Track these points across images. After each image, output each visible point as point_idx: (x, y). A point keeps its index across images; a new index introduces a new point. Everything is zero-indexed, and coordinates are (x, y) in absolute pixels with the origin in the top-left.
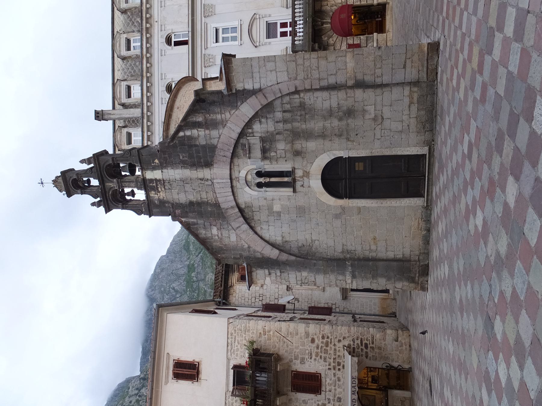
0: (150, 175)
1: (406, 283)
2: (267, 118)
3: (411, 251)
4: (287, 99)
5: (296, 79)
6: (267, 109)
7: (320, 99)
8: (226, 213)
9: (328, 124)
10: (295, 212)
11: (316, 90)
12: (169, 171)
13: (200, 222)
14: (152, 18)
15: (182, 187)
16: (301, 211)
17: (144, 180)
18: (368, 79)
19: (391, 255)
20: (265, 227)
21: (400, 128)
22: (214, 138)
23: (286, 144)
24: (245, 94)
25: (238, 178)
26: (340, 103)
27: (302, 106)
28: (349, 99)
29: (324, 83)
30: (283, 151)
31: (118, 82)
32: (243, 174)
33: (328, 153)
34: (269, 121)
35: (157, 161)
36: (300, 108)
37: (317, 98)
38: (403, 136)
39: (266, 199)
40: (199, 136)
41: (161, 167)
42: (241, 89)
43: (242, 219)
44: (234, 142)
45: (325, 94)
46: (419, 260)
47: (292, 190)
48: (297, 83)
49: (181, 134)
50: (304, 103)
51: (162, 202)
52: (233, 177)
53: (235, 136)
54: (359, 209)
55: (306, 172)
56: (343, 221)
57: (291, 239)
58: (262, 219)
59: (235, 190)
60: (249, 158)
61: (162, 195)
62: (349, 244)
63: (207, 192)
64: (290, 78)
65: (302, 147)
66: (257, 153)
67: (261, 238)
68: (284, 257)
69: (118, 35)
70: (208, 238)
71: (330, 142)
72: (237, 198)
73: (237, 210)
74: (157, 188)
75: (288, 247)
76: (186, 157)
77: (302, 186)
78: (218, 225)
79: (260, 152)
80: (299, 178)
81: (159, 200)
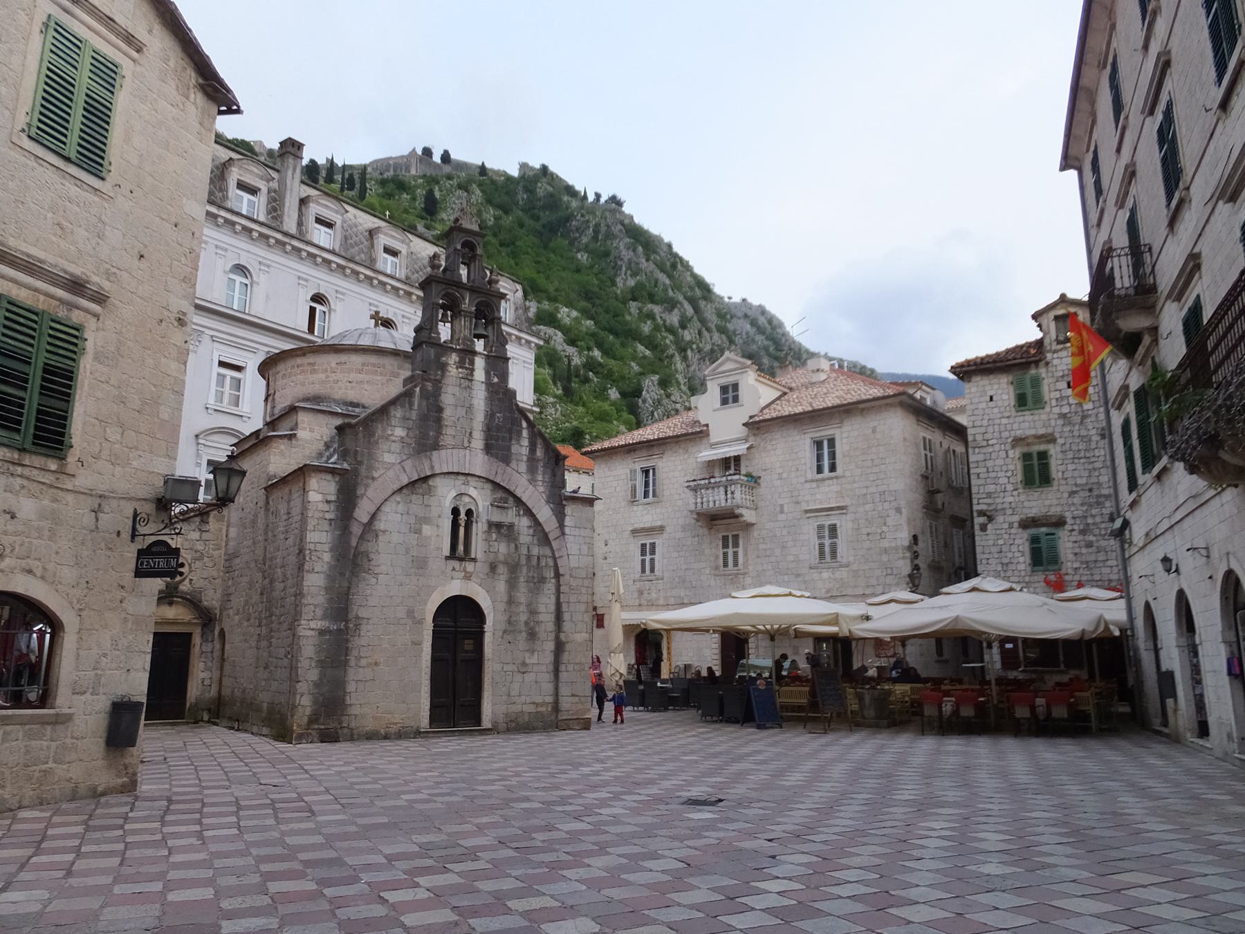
0: (480, 363)
1: (308, 711)
4: (551, 563)
6: (545, 539)
9: (522, 608)
11: (558, 598)
13: (414, 415)
16: (420, 564)
18: (565, 657)
20: (401, 508)
25: (466, 484)
27: (542, 580)
29: (564, 608)
35: (496, 380)
45: (552, 608)
48: (567, 577)
49: (524, 424)
51: (443, 367)
52: (469, 478)
53: (518, 493)
54: (417, 644)
56: (403, 621)
57: (381, 544)
61: (453, 371)
62: (370, 627)
66: (497, 517)
68: (356, 530)
70: (388, 419)
75: (369, 536)
78: (409, 441)
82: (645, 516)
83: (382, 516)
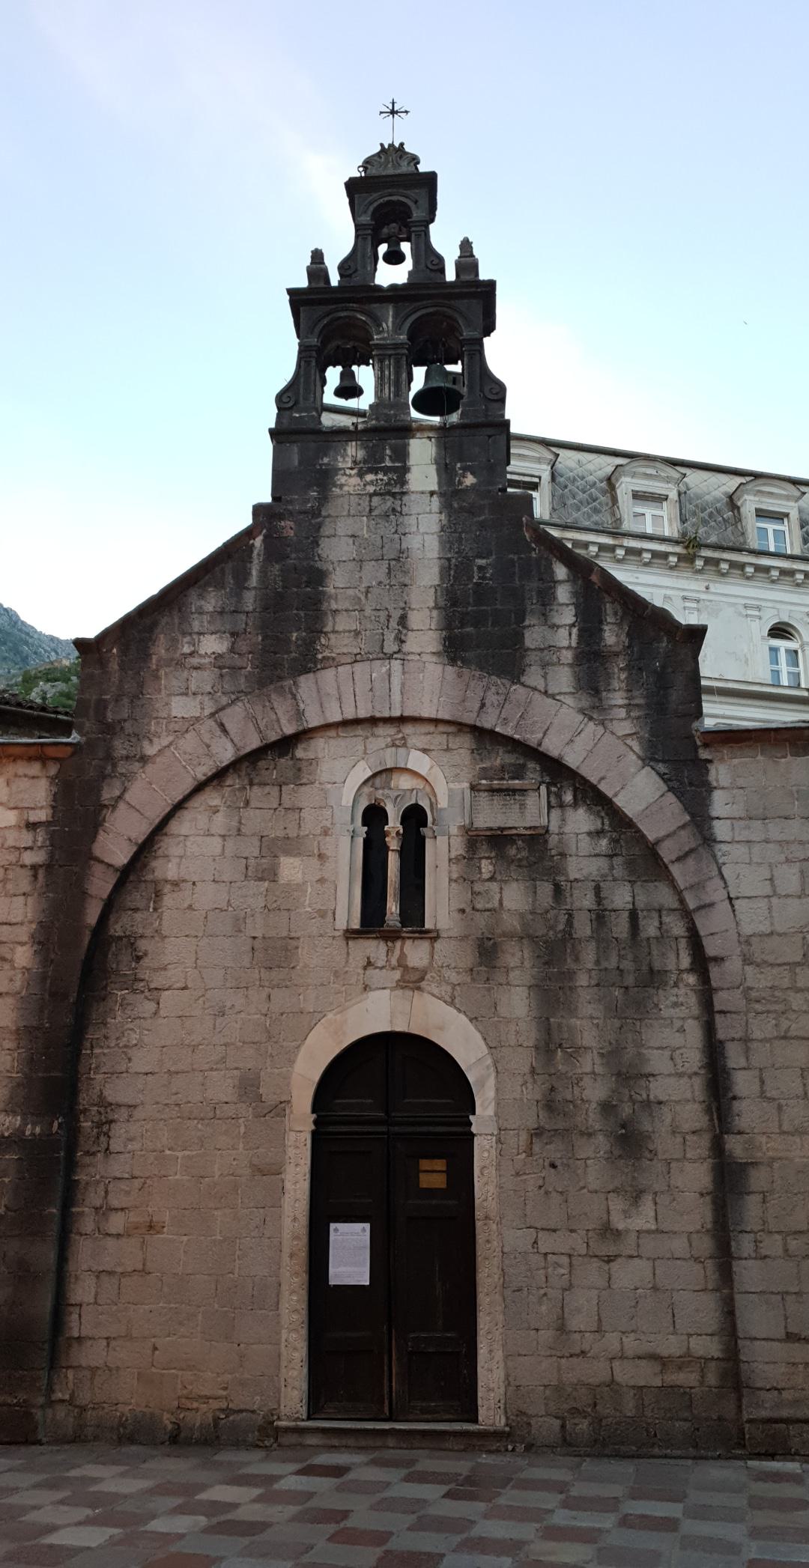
0: (422, 453)
2: (611, 856)
3: (94, 1370)
4: (678, 928)
5: (747, 960)
6: (643, 858)
7: (677, 1040)
8: (281, 691)
9: (589, 1063)
10: (272, 933)
12: (436, 517)
13: (249, 601)
14: (715, 578)
15: (378, 554)
16: (275, 955)
17: (408, 430)
19: (82, 1291)
21: (575, 1323)
22: (545, 677)
23: (522, 916)
26: (665, 1109)
27: (653, 978)
28: (679, 1139)
29: (734, 1057)
30: (497, 904)
31: (551, 457)
32: (418, 761)
33: (489, 1061)
34: (603, 863)
35: (470, 480)
36: (645, 968)
37: (682, 1030)
38: (547, 1335)
40: (555, 627)
41: (449, 494)
42: (712, 777)
43: (254, 743)
44: (532, 739)
45: (693, 1057)
46: (51, 1403)
47: (356, 924)
48: (734, 965)
49: (561, 572)
50: (663, 984)
51: (324, 479)
52: (408, 729)
53: (552, 746)
54: (271, 1171)
55: (422, 979)
56: (229, 1110)
57: (166, 916)
58: (248, 813)
59: (359, 731)
60: (473, 788)
61: (349, 482)
63: (357, 633)
64: (748, 943)
65: (507, 970)
66: (492, 815)
67: (179, 806)
69: (677, 475)
70: (184, 619)
71: (526, 1069)
72: (332, 733)
73: (289, 729)
74: (374, 471)
75: (136, 897)
76: (483, 578)
77: (369, 964)
79: (495, 825)
80: (397, 952)
83: (169, 846)
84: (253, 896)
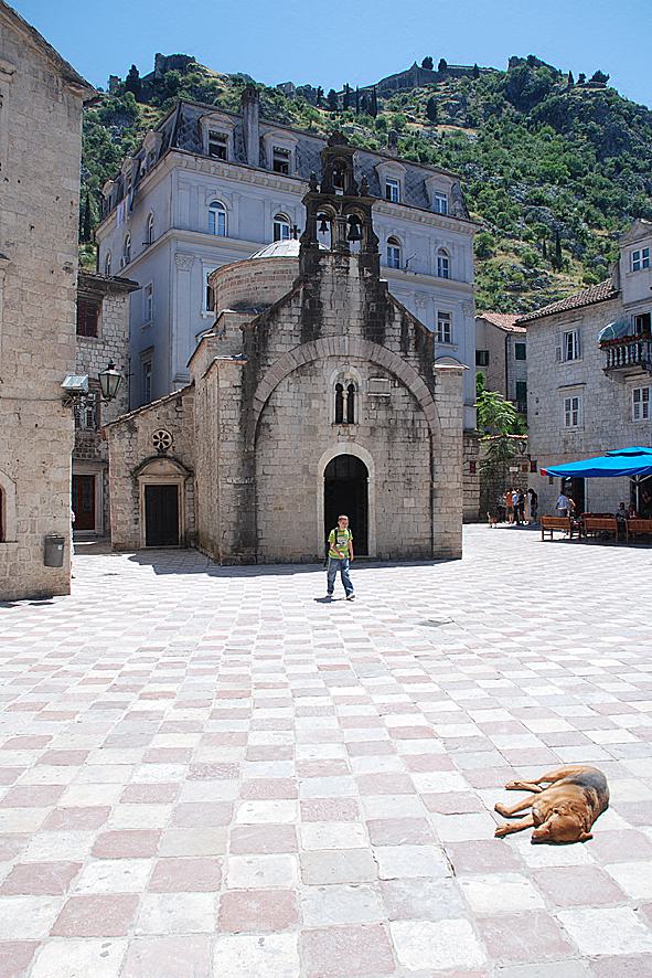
16: (312, 430)
18: (437, 502)
24: (431, 384)
35: (369, 274)
39: (325, 392)
51: (320, 268)
52: (349, 359)
53: (393, 368)
56: (301, 476)
68: (257, 407)
81: (325, 266)
82: (569, 372)
83: (279, 395)
84: (304, 412)
